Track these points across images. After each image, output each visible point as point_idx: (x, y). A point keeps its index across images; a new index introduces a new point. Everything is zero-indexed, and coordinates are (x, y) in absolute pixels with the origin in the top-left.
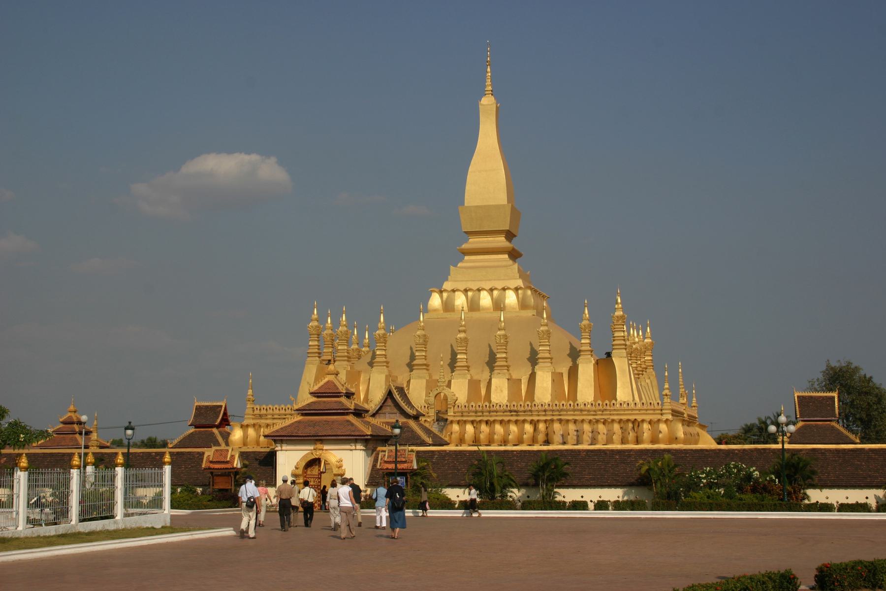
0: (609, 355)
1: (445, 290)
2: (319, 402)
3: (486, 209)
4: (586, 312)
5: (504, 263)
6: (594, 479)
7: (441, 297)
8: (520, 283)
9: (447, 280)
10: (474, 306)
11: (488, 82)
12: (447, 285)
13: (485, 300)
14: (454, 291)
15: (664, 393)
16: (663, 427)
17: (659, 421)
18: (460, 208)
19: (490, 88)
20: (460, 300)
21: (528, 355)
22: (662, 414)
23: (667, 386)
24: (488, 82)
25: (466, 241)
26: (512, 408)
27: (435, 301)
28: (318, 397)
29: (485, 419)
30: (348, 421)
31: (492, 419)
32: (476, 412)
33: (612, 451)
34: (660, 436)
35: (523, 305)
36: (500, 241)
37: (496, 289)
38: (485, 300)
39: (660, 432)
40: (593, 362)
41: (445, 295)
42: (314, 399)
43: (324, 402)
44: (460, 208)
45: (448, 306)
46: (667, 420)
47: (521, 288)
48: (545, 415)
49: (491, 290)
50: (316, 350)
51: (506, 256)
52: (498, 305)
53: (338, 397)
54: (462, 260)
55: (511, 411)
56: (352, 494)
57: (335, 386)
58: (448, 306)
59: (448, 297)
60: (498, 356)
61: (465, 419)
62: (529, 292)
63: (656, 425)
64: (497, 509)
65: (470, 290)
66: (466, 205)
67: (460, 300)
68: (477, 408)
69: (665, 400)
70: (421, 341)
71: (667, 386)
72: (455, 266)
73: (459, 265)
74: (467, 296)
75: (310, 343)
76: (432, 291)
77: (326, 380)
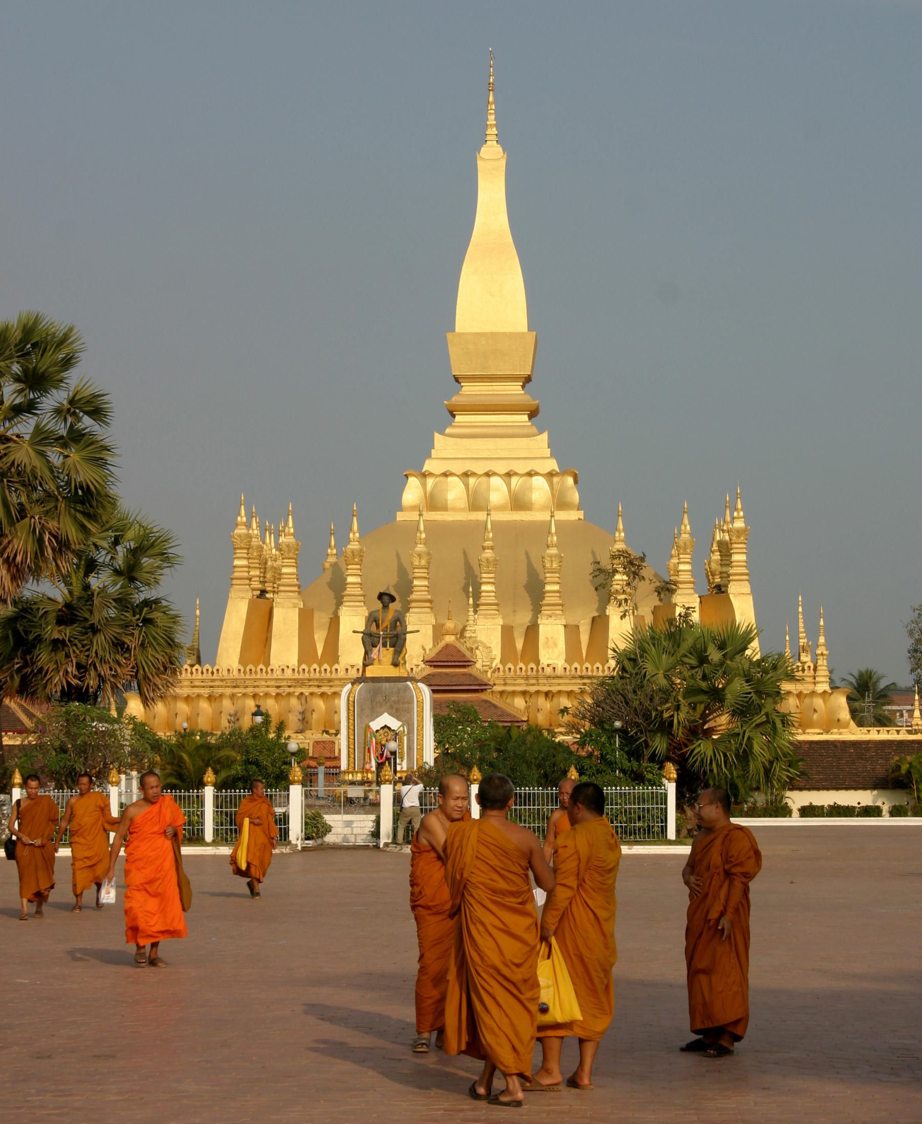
0: (721, 589)
1: (431, 474)
2: (440, 674)
3: (494, 340)
4: (686, 521)
5: (526, 431)
6: (826, 780)
7: (424, 485)
8: (552, 465)
9: (429, 456)
10: (476, 502)
11: (492, 119)
12: (428, 466)
13: (498, 491)
14: (445, 475)
15: (819, 652)
16: (818, 702)
17: (813, 693)
18: (449, 336)
19: (494, 131)
20: (455, 492)
21: (523, 578)
22: (815, 683)
23: (822, 640)
24: (492, 119)
25: (457, 393)
26: (584, 673)
27: (412, 493)
28: (435, 666)
29: (546, 689)
30: (486, 702)
31: (533, 689)
32: (527, 678)
33: (844, 743)
34: (815, 716)
35: (561, 504)
36: (514, 389)
37: (516, 474)
38: (498, 491)
39: (815, 711)
40: (698, 600)
41: (430, 482)
42: (429, 670)
43: (447, 674)
44: (449, 336)
45: (433, 502)
46: (825, 692)
47: (557, 474)
49: (509, 475)
50: (246, 574)
51: (526, 418)
52: (518, 502)
53: (464, 666)
54: (450, 425)
55: (582, 677)
56: (882, 792)
57: (459, 651)
58: (433, 502)
59: (435, 486)
60: (548, 588)
61: (510, 688)
62: (570, 480)
63: (807, 701)
64: (771, 816)
65: (473, 474)
66: (458, 329)
67: (455, 492)
68: (529, 673)
69: (820, 662)
70: (423, 562)
71: (822, 640)
72: (442, 433)
73: (448, 431)
74: (467, 485)
75: (237, 562)
76: (407, 476)
77: (442, 644)
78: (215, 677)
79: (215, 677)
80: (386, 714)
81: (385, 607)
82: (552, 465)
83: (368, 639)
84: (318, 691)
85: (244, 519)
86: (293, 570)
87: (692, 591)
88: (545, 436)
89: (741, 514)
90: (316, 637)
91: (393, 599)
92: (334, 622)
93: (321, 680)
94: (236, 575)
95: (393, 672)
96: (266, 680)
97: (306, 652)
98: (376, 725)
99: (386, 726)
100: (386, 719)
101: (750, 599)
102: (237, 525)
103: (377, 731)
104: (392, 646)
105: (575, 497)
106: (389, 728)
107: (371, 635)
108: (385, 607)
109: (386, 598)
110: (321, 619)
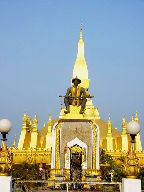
11: (81, 35)
24: (81, 35)
48: (114, 154)
75: (23, 125)
76: (61, 109)
78: (17, 150)
79: (17, 150)
80: (76, 138)
81: (76, 85)
82: (93, 107)
83: (67, 100)
84: (41, 154)
85: (25, 115)
86: (36, 127)
87: (126, 134)
88: (92, 100)
89: (137, 117)
90: (41, 142)
91: (79, 81)
92: (45, 139)
93: (41, 151)
94: (23, 127)
95: (80, 117)
96: (29, 151)
97: (38, 145)
98: (70, 144)
99: (76, 144)
100: (76, 141)
101: (139, 136)
102: (24, 116)
103: (72, 147)
104: (80, 104)
105: (98, 114)
106: (78, 146)
107: (68, 98)
108: (76, 85)
109: (76, 81)
110: (42, 138)
